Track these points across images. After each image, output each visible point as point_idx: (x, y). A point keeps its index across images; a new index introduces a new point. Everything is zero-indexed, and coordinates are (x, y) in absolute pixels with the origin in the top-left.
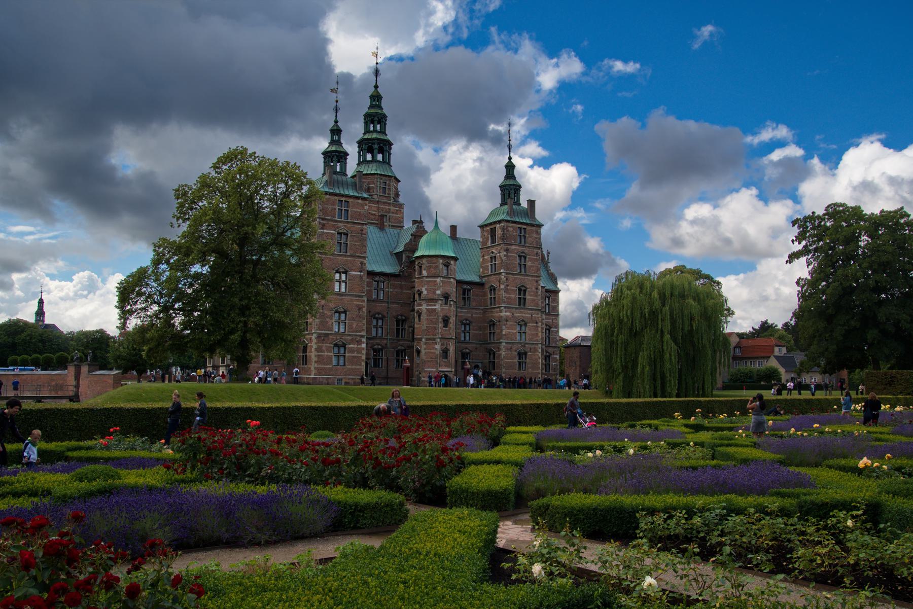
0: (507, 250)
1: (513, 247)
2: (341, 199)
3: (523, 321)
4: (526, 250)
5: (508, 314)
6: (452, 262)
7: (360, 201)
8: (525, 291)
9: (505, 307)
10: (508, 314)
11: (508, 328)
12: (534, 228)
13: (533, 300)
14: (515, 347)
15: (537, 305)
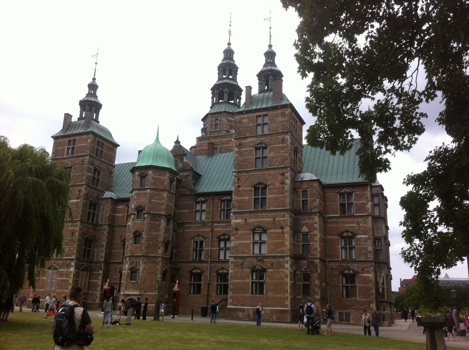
0: (240, 146)
1: (249, 140)
2: (70, 139)
3: (259, 227)
4: (267, 140)
5: (239, 221)
6: (150, 172)
7: (85, 137)
8: (265, 188)
9: (235, 213)
10: (239, 221)
11: (238, 239)
12: (279, 111)
13: (276, 199)
14: (247, 263)
15: (284, 204)
